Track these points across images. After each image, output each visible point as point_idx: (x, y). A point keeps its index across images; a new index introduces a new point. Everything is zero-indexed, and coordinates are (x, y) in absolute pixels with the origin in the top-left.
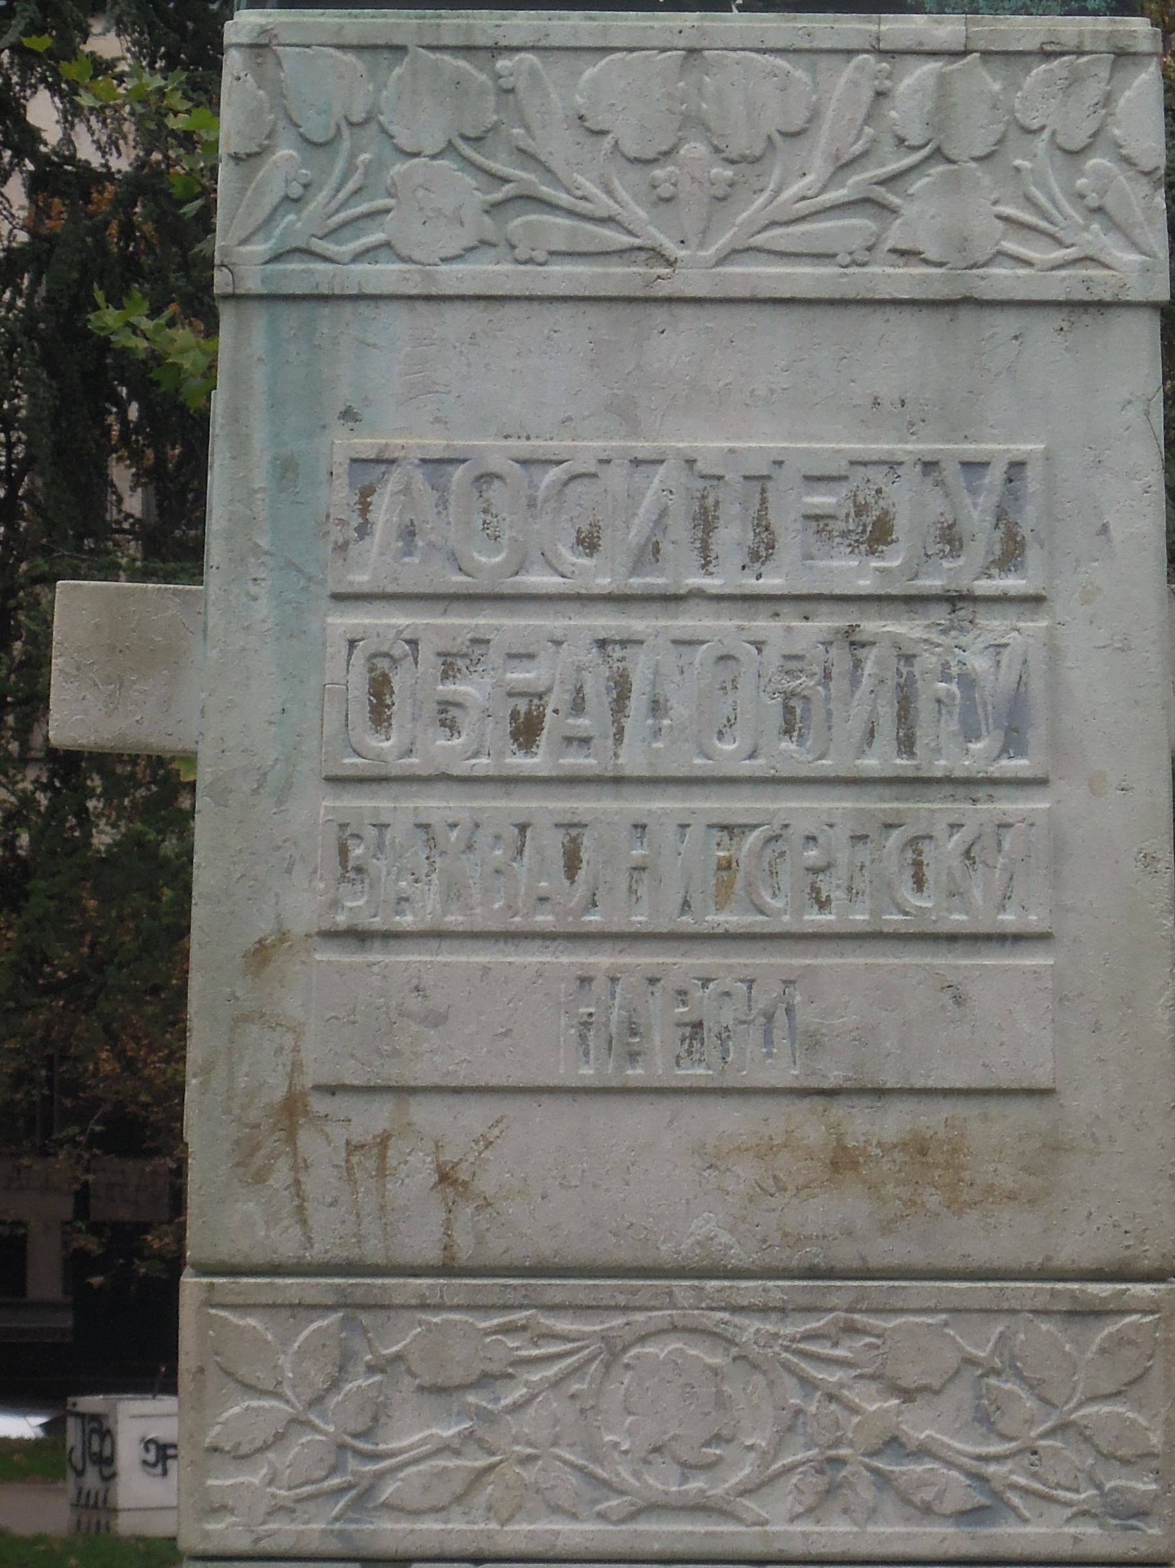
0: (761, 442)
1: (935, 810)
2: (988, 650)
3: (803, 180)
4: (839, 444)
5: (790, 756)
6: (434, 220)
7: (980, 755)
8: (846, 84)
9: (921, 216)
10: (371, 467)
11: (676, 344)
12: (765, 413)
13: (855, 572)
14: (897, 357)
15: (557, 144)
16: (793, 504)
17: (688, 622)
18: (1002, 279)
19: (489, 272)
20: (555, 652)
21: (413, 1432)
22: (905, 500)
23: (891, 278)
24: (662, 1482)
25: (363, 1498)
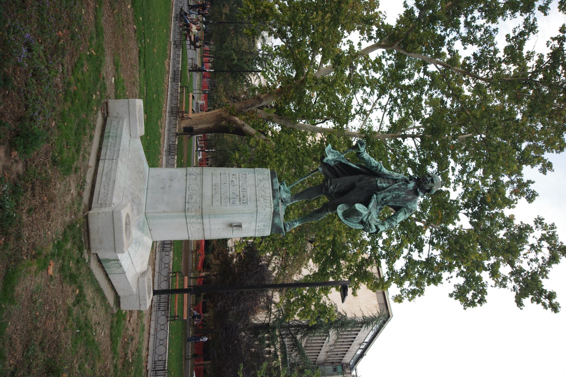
0: (248, 192)
1: (228, 199)
2: (237, 202)
3: (263, 193)
4: (249, 195)
5: (231, 193)
6: (259, 177)
7: (231, 201)
8: (268, 195)
9: (261, 199)
10: (246, 174)
11: (254, 188)
12: (250, 192)
13: (241, 196)
14: (253, 198)
15: (264, 182)
16: (245, 193)
17: (238, 189)
18: (258, 202)
19: (257, 180)
20: (236, 182)
21: (193, 177)
22: (245, 198)
23: (258, 198)
24: (190, 188)
25: (190, 175)
